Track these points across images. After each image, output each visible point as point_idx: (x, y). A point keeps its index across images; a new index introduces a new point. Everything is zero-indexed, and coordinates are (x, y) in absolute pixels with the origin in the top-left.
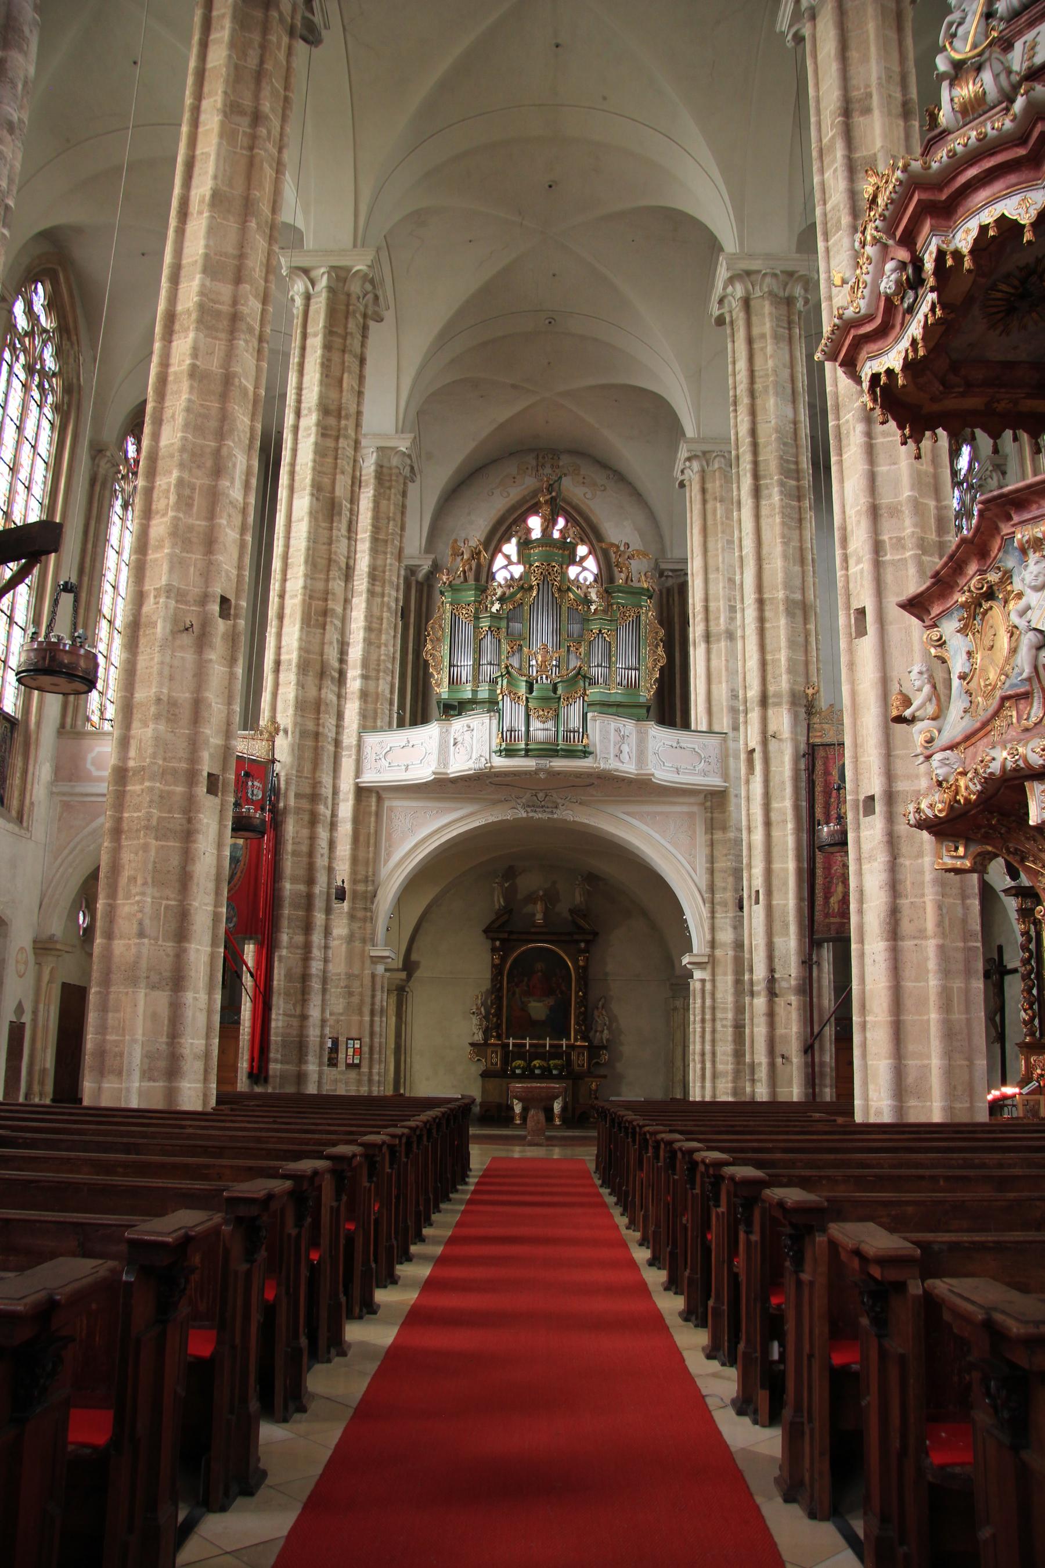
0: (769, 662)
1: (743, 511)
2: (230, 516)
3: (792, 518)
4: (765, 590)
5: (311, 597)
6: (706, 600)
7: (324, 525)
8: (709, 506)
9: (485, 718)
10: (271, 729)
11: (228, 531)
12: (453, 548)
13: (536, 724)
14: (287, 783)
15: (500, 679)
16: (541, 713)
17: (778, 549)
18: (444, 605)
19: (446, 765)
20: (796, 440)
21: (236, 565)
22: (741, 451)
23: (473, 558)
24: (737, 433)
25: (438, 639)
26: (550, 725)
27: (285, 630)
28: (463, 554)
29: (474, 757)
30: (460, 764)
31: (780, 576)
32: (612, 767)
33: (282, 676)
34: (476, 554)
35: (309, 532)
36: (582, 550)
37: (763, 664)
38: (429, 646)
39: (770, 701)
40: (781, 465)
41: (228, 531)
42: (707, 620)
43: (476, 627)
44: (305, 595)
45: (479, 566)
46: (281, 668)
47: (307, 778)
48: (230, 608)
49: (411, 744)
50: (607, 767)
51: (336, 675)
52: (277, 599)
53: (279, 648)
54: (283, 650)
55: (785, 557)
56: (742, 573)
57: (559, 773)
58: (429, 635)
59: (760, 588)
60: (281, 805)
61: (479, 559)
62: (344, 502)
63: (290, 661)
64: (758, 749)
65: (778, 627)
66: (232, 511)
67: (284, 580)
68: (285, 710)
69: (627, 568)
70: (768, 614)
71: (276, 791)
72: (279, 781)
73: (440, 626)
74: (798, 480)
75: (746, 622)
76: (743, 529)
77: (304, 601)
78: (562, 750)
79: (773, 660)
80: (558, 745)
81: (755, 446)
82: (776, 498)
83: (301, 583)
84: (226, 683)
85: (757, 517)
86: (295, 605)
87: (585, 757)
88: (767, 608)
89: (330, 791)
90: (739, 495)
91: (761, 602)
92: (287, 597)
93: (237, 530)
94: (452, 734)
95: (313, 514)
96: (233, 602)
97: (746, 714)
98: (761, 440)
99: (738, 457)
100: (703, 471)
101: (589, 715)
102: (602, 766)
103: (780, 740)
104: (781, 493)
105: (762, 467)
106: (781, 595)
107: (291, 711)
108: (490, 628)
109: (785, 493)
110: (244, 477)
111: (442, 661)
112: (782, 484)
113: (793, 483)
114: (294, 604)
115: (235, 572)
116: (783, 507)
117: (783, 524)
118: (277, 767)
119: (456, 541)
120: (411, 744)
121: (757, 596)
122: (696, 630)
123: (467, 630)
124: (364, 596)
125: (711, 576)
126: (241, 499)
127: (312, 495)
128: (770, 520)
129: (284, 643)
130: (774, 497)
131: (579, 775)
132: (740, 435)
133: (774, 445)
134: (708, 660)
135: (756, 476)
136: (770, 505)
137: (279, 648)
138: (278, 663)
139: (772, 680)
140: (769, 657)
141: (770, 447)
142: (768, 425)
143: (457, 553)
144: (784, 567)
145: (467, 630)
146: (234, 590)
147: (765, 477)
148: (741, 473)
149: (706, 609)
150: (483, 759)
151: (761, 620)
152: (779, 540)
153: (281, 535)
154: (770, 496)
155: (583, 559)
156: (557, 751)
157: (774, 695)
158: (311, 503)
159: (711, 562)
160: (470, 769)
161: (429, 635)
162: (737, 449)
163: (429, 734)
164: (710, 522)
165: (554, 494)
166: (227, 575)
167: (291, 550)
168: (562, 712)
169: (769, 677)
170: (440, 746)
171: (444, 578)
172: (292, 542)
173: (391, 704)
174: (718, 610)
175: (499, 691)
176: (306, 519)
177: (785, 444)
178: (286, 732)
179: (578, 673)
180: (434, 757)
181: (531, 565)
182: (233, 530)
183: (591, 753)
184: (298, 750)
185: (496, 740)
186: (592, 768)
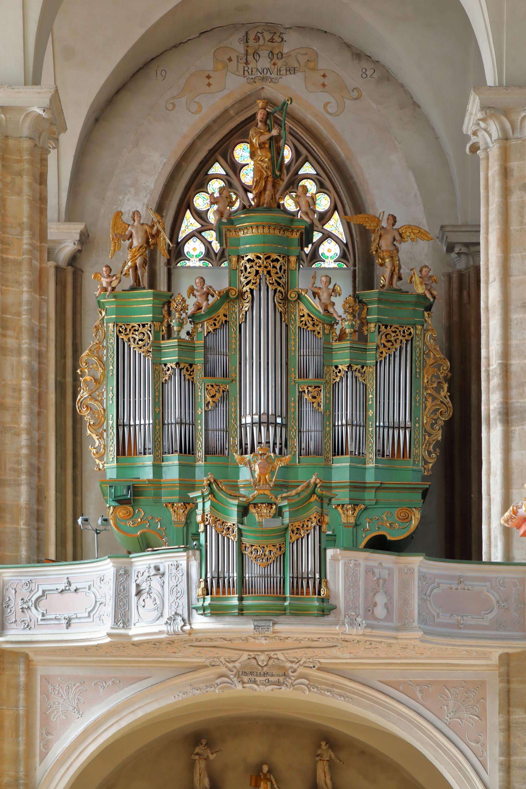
9: (181, 558)
15: (200, 501)
29: (166, 615)
43: (157, 364)
49: (73, 588)
73: (100, 359)
94: (134, 578)
120: (73, 588)
122: (491, 401)
149: (506, 369)
150: (179, 619)
160: (161, 632)
170: (117, 594)
173: (38, 517)
175: (199, 518)
180: (109, 609)
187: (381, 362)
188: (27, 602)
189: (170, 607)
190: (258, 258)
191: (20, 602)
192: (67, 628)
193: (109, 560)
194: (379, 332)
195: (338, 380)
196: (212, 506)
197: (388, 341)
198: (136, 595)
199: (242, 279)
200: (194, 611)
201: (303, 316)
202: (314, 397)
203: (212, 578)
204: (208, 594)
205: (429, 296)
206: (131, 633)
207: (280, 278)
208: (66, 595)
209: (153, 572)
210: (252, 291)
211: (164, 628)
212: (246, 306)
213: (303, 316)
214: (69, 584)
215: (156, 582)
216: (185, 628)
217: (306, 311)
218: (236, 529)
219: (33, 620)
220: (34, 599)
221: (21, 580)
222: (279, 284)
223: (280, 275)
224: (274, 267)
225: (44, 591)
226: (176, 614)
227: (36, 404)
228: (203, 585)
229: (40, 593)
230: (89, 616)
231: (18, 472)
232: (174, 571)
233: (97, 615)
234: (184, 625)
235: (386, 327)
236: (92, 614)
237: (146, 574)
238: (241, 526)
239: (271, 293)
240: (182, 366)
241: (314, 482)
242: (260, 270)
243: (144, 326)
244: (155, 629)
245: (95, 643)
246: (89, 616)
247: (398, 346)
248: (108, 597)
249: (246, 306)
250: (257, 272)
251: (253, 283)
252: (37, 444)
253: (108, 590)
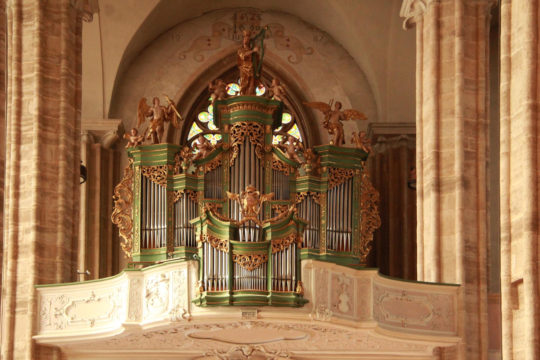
12: (140, 107)
18: (133, 164)
23: (165, 119)
25: (127, 203)
28: (152, 114)
34: (167, 116)
36: (287, 118)
38: (117, 210)
43: (171, 192)
45: (172, 129)
58: (117, 199)
61: (171, 120)
69: (338, 129)
73: (130, 189)
108: (185, 190)
111: (133, 225)
119: (144, 101)
123: (160, 194)
124: (35, 142)
143: (146, 113)
145: (160, 194)
155: (288, 127)
161: (117, 199)
165: (255, 49)
171: (132, 139)
181: (230, 126)
190: (243, 124)
199: (232, 139)
210: (239, 145)
240: (188, 192)
242: (245, 132)
243: (161, 167)
249: (235, 155)
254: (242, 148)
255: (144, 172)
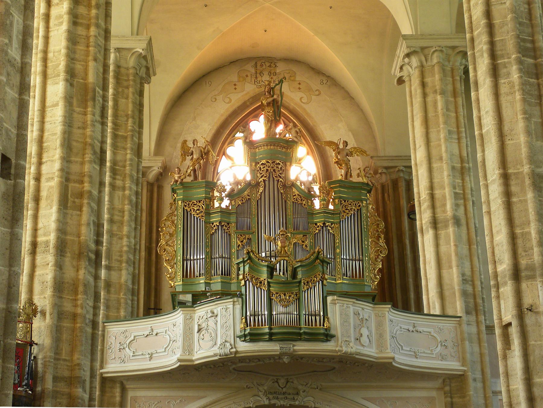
0: (519, 236)
1: (481, 91)
2: (8, 74)
3: (532, 95)
4: (510, 165)
5: (67, 180)
6: (432, 188)
7: (78, 109)
8: (429, 99)
10: (29, 311)
11: (8, 89)
13: (278, 309)
14: (45, 365)
16: (283, 297)
17: (521, 125)
19: (191, 352)
20: (531, 20)
21: (15, 124)
22: (475, 33)
24: (470, 17)
26: (292, 308)
27: (42, 212)
28: (192, 154)
29: (219, 342)
30: (204, 351)
31: (524, 151)
32: (353, 350)
33: (39, 259)
35: (65, 117)
37: (513, 238)
39: (523, 274)
40: (518, 43)
41: (8, 89)
42: (433, 207)
44: (61, 177)
46: (38, 250)
47: (65, 360)
48: (10, 168)
49: (154, 333)
50: (349, 350)
51: (93, 256)
52: (32, 182)
53: (35, 230)
54: (40, 232)
55: (528, 133)
56: (483, 151)
57: (302, 357)
59: (503, 163)
60: (39, 389)
62: (97, 88)
63: (47, 243)
64: (515, 323)
65: (526, 201)
66: (10, 69)
67: (40, 163)
68: (42, 292)
70: (514, 189)
71: (33, 375)
72: (36, 364)
73: (173, 222)
74: (535, 58)
75: (491, 197)
76: (482, 108)
77: (61, 183)
78: (305, 333)
79: (522, 234)
80: (300, 329)
81: (491, 28)
82: (515, 76)
83: (57, 165)
84: (7, 244)
85: (497, 95)
86: (51, 187)
87: (327, 340)
88: (513, 182)
89: (88, 373)
90: (476, 76)
91: (506, 178)
92: (43, 179)
93: (16, 89)
94: (196, 321)
95: (68, 99)
96: (13, 161)
97: (498, 288)
98: (497, 21)
99: (472, 40)
100: (422, 66)
101: (329, 299)
102: (344, 349)
103: (537, 313)
104: (520, 70)
105: (498, 47)
106: (526, 169)
107: (49, 292)
108: (220, 223)
109: (524, 71)
110: (21, 37)
111: (176, 256)
112: (520, 62)
113: (531, 61)
114: (51, 186)
115: (14, 131)
116: (523, 84)
117: (524, 100)
118: (35, 349)
119: (185, 142)
120: (154, 333)
121: (501, 171)
125: (435, 165)
126: (18, 58)
127: (67, 80)
128: (510, 98)
129: (40, 225)
130: (513, 75)
131: (320, 359)
132: (474, 18)
133: (510, 26)
134: (437, 245)
135: (493, 56)
136: (509, 83)
137: (35, 230)
138: (34, 245)
139: (524, 254)
140: (518, 231)
141: (506, 27)
142: (504, 6)
144: (527, 142)
146: (14, 149)
147: (502, 57)
148: (477, 55)
151: (507, 194)
152: (520, 117)
153: (36, 120)
154: (508, 74)
156: (300, 334)
157: (526, 269)
158: (66, 88)
159: (434, 152)
160: (215, 355)
162: (472, 31)
163: (172, 323)
164: (431, 114)
166: (7, 135)
167: (46, 134)
168: (305, 296)
169: (520, 251)
170: (185, 333)
172: (47, 126)
174: (444, 197)
176: (61, 104)
177: (520, 24)
178: (43, 313)
179: (317, 258)
180: (180, 343)
182: (12, 88)
183: (333, 336)
184: (57, 331)
185: (240, 326)
186: (335, 351)
187: (343, 221)
188: (123, 345)
189: (221, 338)
191: (118, 345)
192: (150, 361)
193: (180, 309)
194: (341, 204)
195: (317, 231)
196: (250, 268)
197: (346, 209)
198: (198, 332)
200: (238, 339)
201: (295, 195)
202: (303, 242)
203: (251, 315)
204: (247, 327)
205: (370, 183)
206: (194, 358)
207: (281, 174)
208: (149, 338)
209: (210, 315)
210: (264, 181)
211: (218, 352)
212: (261, 190)
213: (295, 195)
214: (152, 330)
215: (211, 322)
216: (232, 350)
217: (297, 193)
218: (266, 283)
219: (127, 357)
220: (128, 342)
221: (119, 330)
222: (280, 177)
223: (280, 172)
224: (277, 167)
225: (135, 337)
226: (226, 341)
227: (134, 223)
228: (244, 320)
229: (132, 338)
230: (165, 351)
231: (121, 262)
232: (224, 313)
233: (171, 349)
234: (232, 348)
235: (345, 201)
236: (167, 350)
237: (205, 317)
238: (269, 280)
239: (276, 183)
241: (318, 251)
242: (269, 169)
243: (200, 202)
244: (211, 354)
245: (169, 369)
246: (165, 351)
247: (352, 213)
248: (178, 335)
249: (261, 190)
250: (267, 170)
251: (265, 177)
252: (133, 247)
253: (179, 330)
254: (267, 183)
255: (186, 206)
